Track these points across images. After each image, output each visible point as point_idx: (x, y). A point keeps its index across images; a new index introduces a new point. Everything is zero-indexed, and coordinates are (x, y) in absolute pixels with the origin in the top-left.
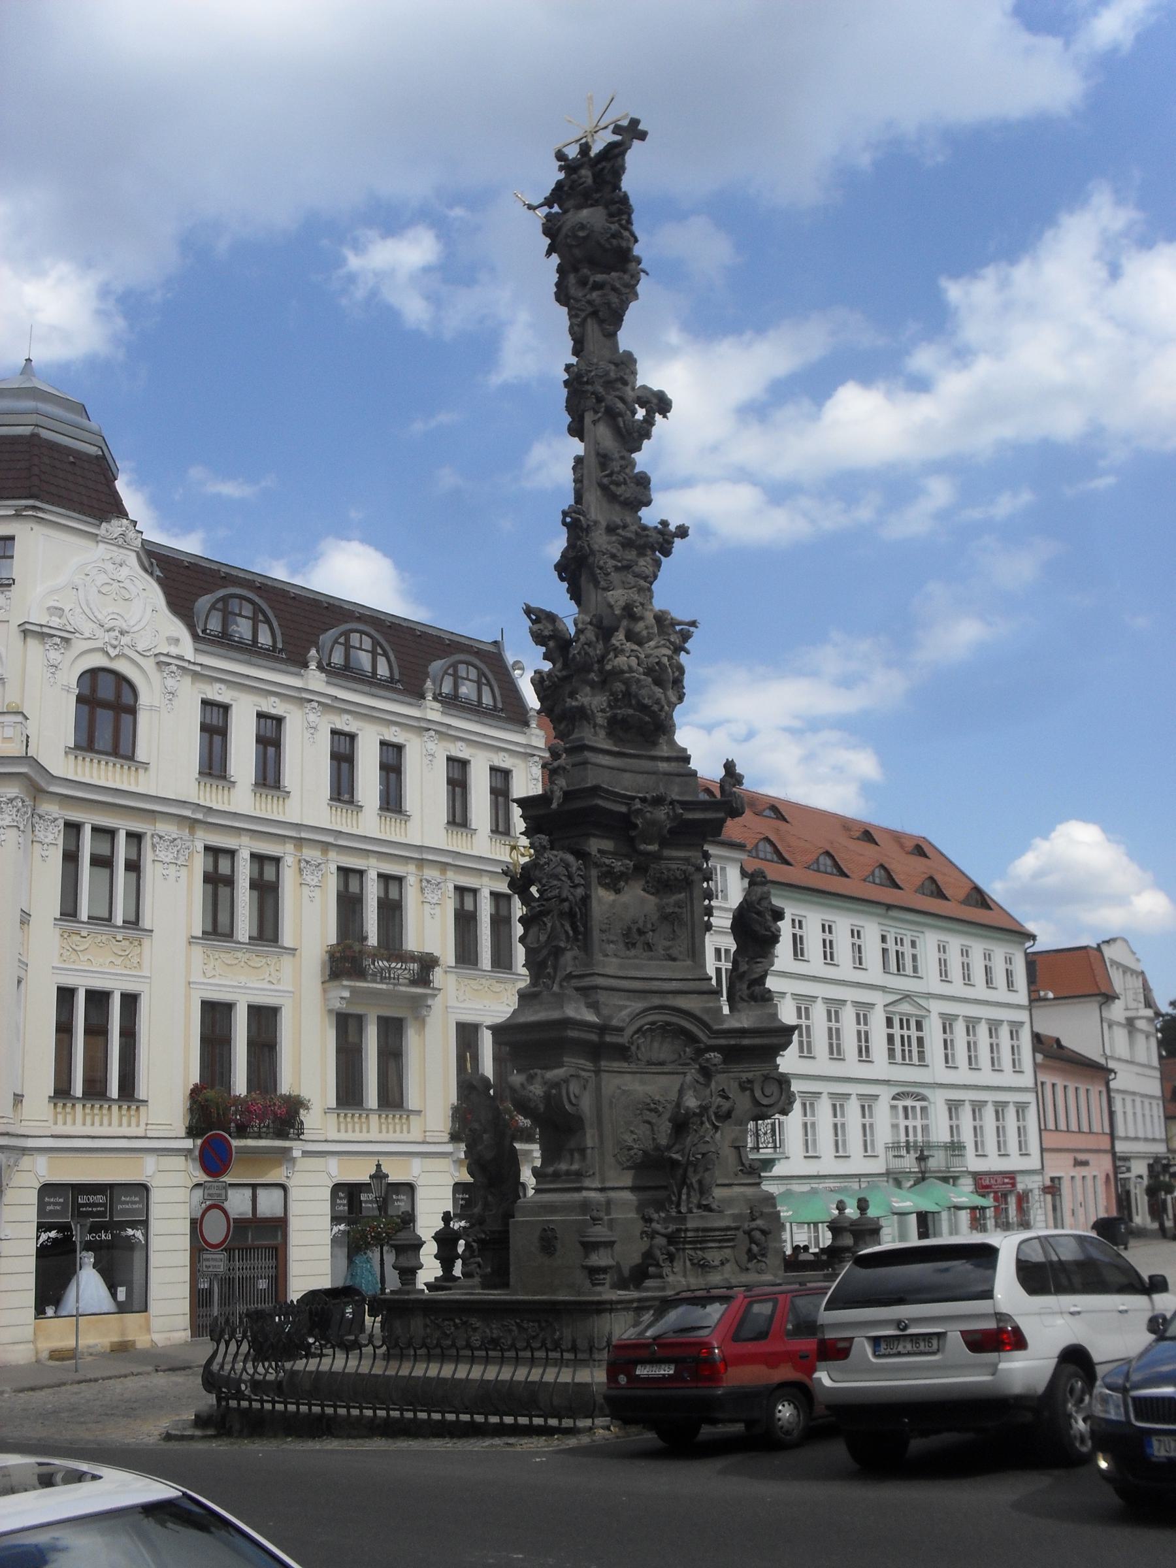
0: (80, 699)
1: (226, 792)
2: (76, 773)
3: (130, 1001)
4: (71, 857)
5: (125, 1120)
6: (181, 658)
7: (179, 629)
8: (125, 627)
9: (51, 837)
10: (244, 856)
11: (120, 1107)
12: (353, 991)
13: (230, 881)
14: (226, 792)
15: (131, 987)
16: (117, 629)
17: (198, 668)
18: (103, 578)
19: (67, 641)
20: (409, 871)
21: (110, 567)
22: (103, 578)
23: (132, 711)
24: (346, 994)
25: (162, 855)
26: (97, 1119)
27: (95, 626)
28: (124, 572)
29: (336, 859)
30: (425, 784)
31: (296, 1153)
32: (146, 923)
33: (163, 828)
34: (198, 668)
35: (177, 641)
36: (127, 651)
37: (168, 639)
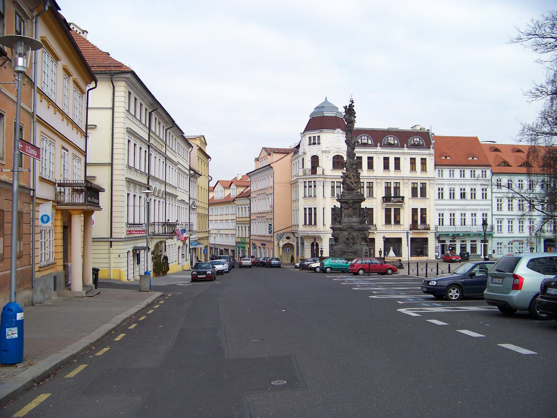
4: (333, 187)
10: (365, 183)
13: (363, 187)
29: (384, 181)
30: (405, 164)
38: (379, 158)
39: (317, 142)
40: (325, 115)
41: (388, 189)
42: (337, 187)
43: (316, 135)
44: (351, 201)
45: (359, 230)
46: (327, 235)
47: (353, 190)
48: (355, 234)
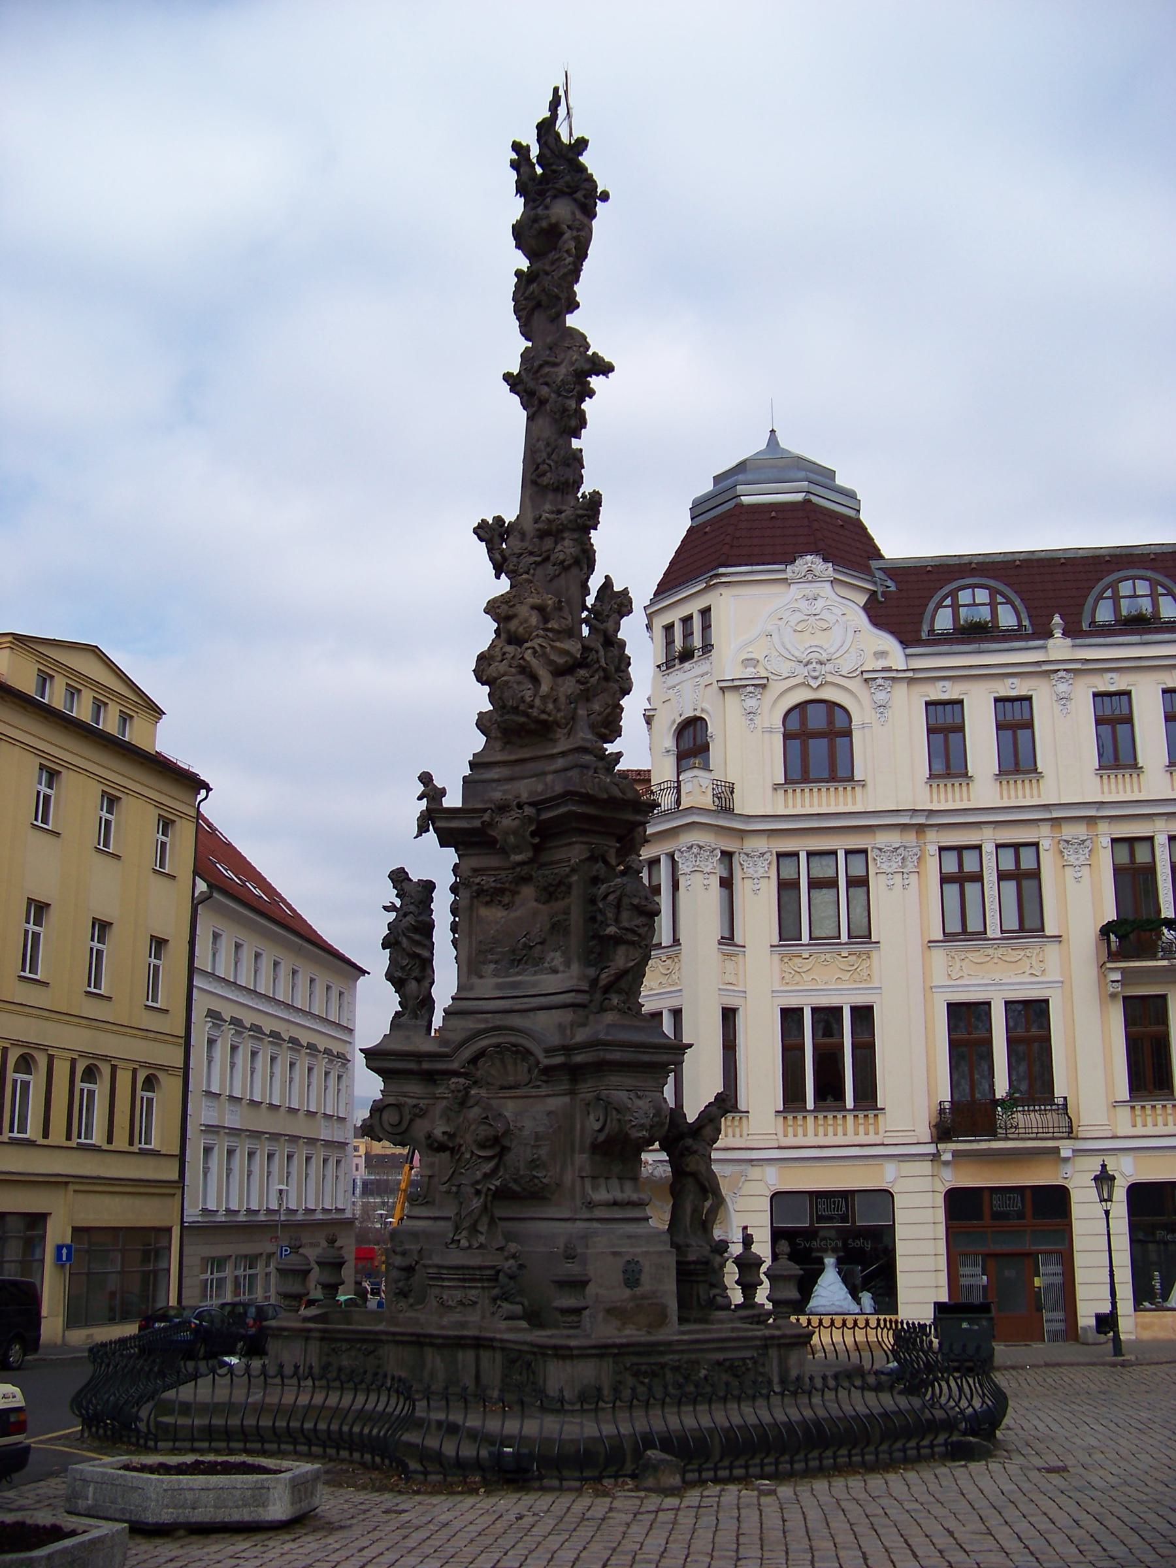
0: (787, 736)
1: (964, 788)
2: (786, 806)
3: (864, 1015)
4: (787, 887)
5: (861, 1128)
6: (890, 670)
7: (888, 642)
8: (824, 657)
9: (761, 870)
10: (988, 848)
11: (816, 1117)
12: (1124, 971)
13: (978, 878)
14: (964, 788)
15: (861, 1000)
16: (814, 661)
17: (910, 674)
18: (799, 616)
19: (764, 686)
20: (1044, 835)
21: (803, 605)
22: (799, 616)
23: (848, 733)
24: (1117, 976)
25: (885, 867)
26: (830, 1129)
27: (793, 664)
28: (820, 604)
29: (1106, 832)
31: (1064, 1153)
32: (738, 939)
33: (884, 839)
34: (910, 674)
35: (882, 654)
36: (829, 678)
37: (875, 654)
38: (1064, 699)
39: (697, 641)
40: (745, 500)
41: (1134, 879)
42: (814, 884)
43: (693, 608)
44: (507, 822)
45: (575, 1073)
46: (754, 1172)
47: (543, 730)
48: (531, 1114)
